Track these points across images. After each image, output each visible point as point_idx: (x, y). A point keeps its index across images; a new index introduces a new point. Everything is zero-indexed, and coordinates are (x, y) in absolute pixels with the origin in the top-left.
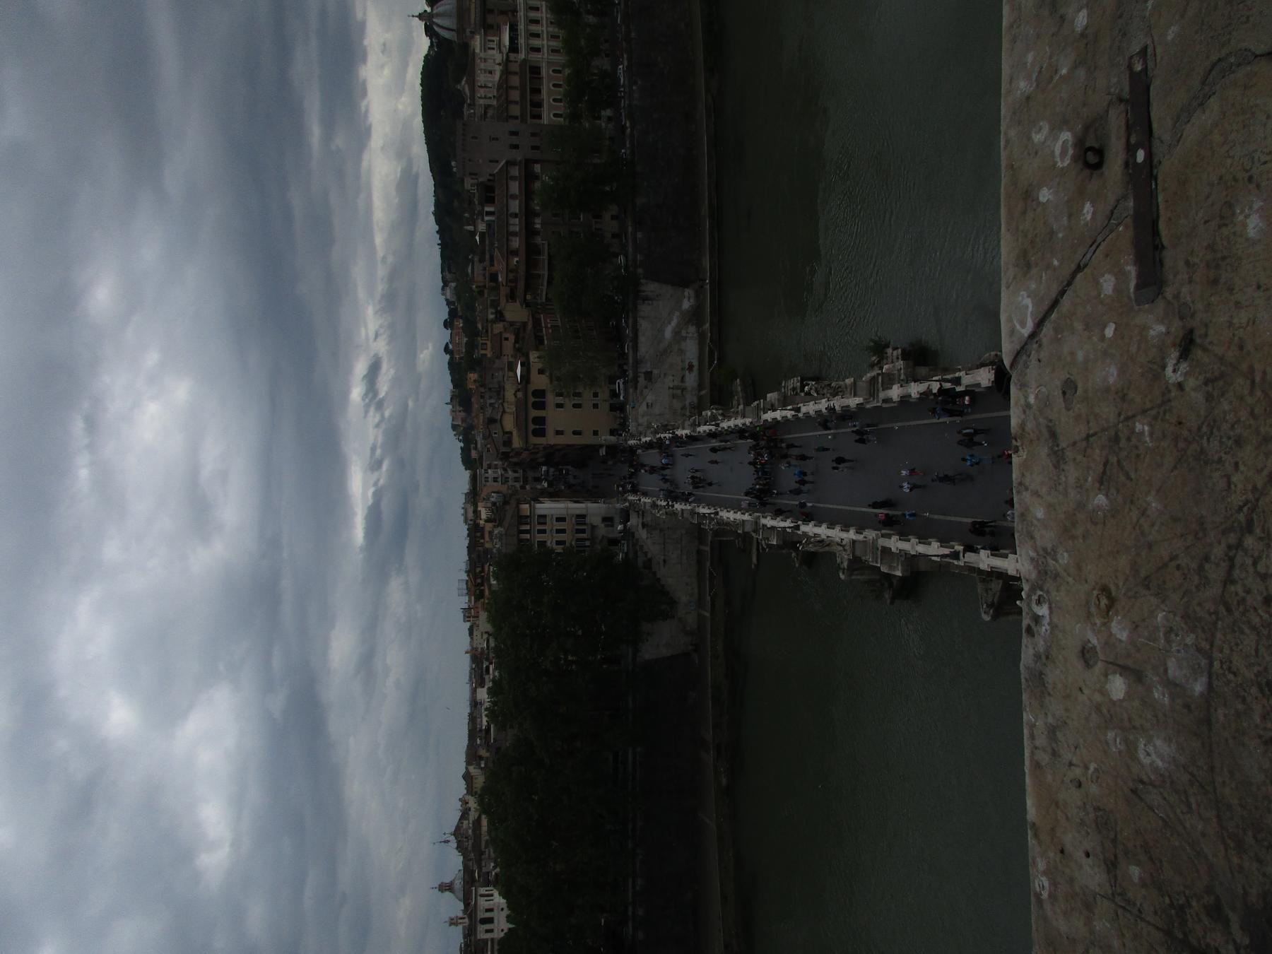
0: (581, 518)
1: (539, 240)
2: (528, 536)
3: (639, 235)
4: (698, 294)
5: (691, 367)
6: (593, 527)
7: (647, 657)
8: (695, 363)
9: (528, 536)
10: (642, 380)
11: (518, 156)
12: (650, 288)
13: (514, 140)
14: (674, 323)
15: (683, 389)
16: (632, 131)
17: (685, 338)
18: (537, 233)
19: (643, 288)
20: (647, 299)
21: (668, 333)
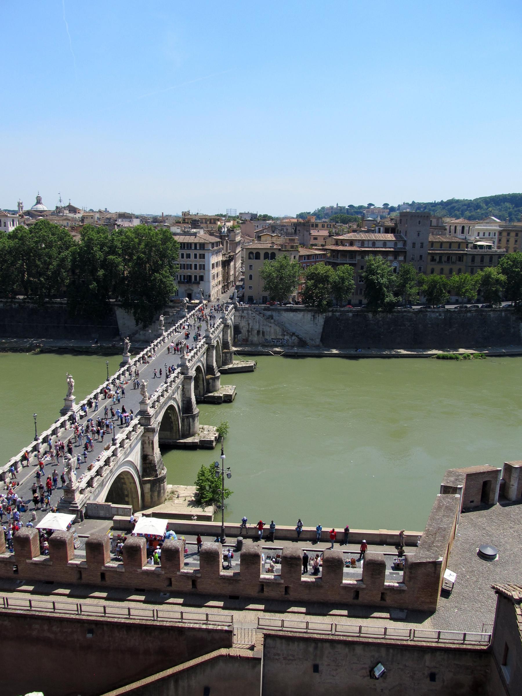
1: (358, 258)
2: (193, 247)
3: (351, 314)
7: (117, 312)
9: (193, 247)
11: (409, 247)
12: (321, 319)
13: (418, 245)
18: (363, 258)
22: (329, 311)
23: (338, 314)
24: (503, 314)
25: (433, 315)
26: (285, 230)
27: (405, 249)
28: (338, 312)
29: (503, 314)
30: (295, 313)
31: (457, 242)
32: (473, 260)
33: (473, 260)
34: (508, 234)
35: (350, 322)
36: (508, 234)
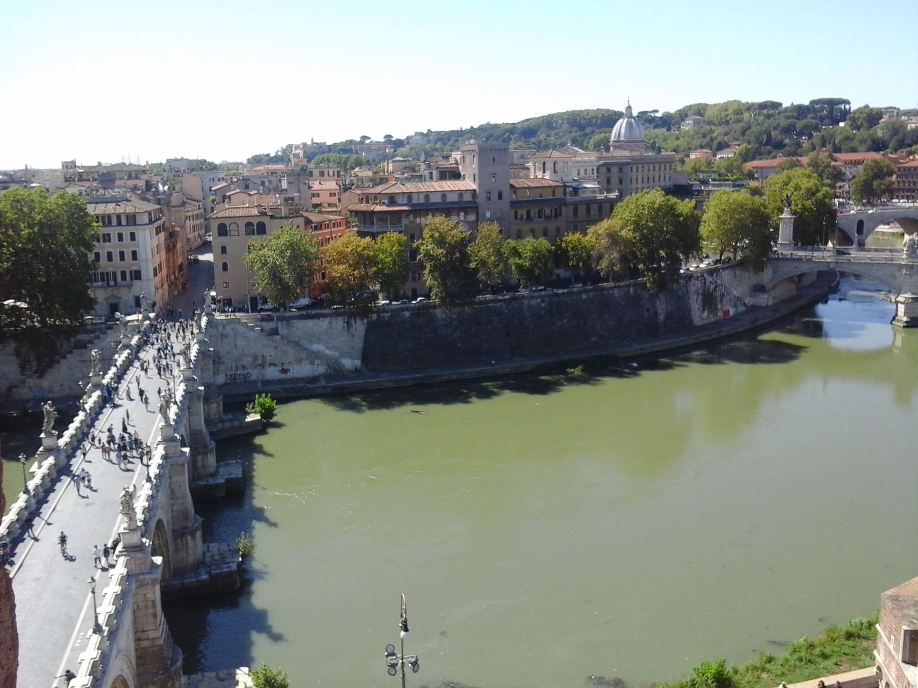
0: (137, 275)
3: (407, 314)
4: (356, 371)
5: (284, 371)
6: (130, 287)
8: (289, 375)
10: (269, 325)
12: (360, 327)
14: (327, 352)
15: (262, 366)
16: (501, 300)
17: (312, 363)
19: (358, 320)
20: (348, 324)
21: (316, 347)
22: (373, 312)
23: (387, 315)
24: (631, 289)
25: (533, 302)
26: (267, 184)
27: (475, 202)
28: (387, 312)
29: (631, 289)
30: (315, 321)
31: (550, 187)
32: (576, 211)
33: (576, 211)
34: (609, 170)
35: (408, 326)
36: (609, 170)
